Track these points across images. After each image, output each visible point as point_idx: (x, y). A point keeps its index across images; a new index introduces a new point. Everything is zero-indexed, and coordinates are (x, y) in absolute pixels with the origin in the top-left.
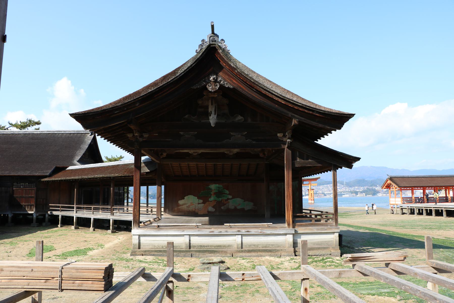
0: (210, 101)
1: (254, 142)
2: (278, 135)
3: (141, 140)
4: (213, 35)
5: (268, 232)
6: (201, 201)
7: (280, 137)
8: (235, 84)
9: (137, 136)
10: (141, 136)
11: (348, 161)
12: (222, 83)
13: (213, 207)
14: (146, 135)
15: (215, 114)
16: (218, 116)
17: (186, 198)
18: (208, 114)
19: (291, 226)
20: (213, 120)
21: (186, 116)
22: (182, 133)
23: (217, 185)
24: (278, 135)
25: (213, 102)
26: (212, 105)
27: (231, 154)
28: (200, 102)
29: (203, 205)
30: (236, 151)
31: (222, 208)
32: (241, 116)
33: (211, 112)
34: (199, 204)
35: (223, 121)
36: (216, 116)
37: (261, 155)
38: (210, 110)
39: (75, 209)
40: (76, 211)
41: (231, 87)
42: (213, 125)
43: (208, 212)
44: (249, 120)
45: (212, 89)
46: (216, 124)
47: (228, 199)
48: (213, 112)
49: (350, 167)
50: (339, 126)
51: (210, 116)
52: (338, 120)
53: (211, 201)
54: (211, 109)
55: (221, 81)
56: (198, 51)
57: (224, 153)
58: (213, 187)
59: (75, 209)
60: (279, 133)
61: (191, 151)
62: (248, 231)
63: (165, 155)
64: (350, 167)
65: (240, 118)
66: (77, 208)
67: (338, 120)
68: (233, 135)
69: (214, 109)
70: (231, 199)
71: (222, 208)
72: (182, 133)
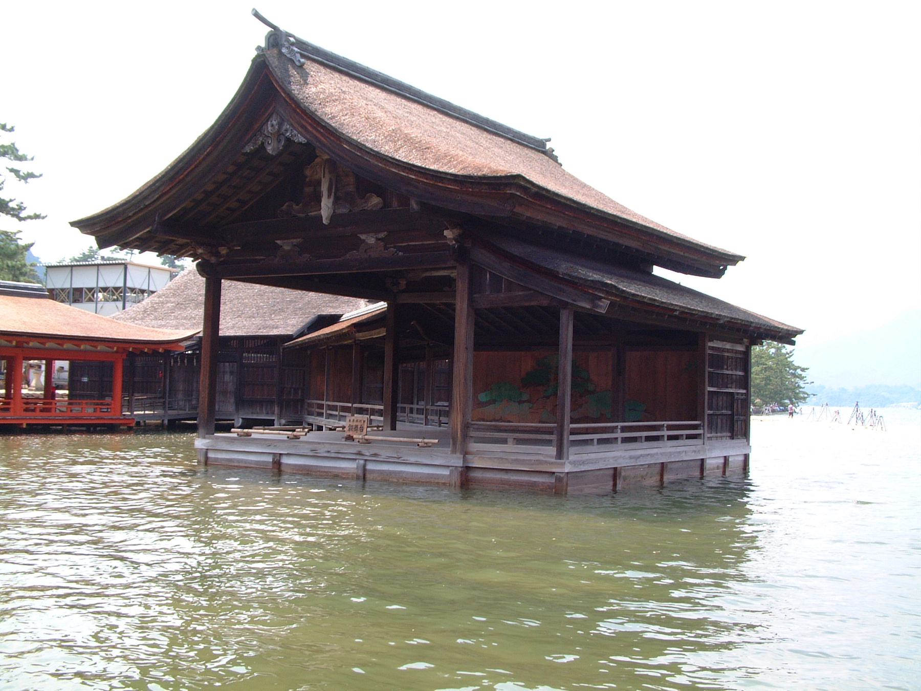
2: (446, 233)
5: (413, 460)
10: (217, 254)
14: (224, 251)
15: (329, 197)
20: (326, 208)
21: (284, 207)
22: (278, 242)
24: (446, 233)
25: (327, 171)
28: (308, 172)
34: (520, 402)
35: (343, 211)
36: (331, 200)
41: (302, 139)
45: (273, 150)
46: (334, 217)
63: (403, 283)
72: (278, 242)
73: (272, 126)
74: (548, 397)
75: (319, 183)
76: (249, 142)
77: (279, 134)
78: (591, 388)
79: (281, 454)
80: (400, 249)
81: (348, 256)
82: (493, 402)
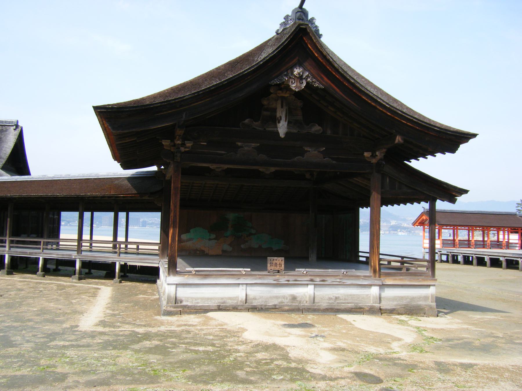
0: (279, 102)
1: (334, 162)
3: (183, 149)
4: (300, 10)
6: (213, 236)
7: (368, 157)
8: (326, 82)
9: (179, 144)
10: (183, 145)
11: (451, 193)
12: (309, 80)
13: (230, 245)
14: (189, 144)
15: (286, 121)
16: (289, 123)
17: (192, 231)
18: (275, 120)
19: (377, 275)
20: (282, 128)
21: (247, 121)
22: (239, 144)
23: (237, 214)
25: (284, 104)
26: (282, 107)
27: (268, 172)
28: (265, 102)
29: (216, 241)
30: (273, 169)
31: (242, 246)
32: (319, 125)
33: (281, 117)
34: (210, 239)
35: (295, 131)
36: (287, 123)
37: (308, 176)
38: (278, 115)
39: (7, 245)
40: (10, 247)
41: (321, 86)
42: (282, 135)
43: (224, 251)
44: (329, 132)
45: (296, 87)
46: (287, 134)
47: (251, 234)
48: (283, 118)
49: (453, 200)
50: (453, 149)
51: (279, 122)
52: (450, 140)
53: (227, 237)
54: (281, 113)
55: (308, 77)
56: (279, 32)
57: (208, 167)
58: (231, 216)
59: (7, 245)
60: (366, 151)
61: (212, 166)
62: (323, 281)
64: (453, 200)
65: (316, 128)
66: (12, 242)
67: (450, 140)
68: (307, 151)
69: (284, 113)
70: (255, 234)
71: (242, 246)
72: (239, 144)
73: (297, 71)
74: (227, 237)
75: (275, 110)
76: (277, 77)
77: (300, 78)
78: (253, 231)
79: (247, 284)
80: (333, 159)
81: (295, 159)
82: (190, 239)
